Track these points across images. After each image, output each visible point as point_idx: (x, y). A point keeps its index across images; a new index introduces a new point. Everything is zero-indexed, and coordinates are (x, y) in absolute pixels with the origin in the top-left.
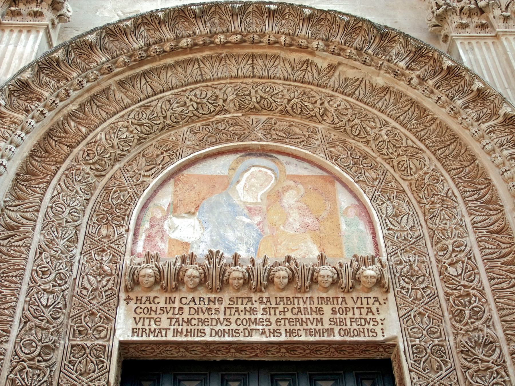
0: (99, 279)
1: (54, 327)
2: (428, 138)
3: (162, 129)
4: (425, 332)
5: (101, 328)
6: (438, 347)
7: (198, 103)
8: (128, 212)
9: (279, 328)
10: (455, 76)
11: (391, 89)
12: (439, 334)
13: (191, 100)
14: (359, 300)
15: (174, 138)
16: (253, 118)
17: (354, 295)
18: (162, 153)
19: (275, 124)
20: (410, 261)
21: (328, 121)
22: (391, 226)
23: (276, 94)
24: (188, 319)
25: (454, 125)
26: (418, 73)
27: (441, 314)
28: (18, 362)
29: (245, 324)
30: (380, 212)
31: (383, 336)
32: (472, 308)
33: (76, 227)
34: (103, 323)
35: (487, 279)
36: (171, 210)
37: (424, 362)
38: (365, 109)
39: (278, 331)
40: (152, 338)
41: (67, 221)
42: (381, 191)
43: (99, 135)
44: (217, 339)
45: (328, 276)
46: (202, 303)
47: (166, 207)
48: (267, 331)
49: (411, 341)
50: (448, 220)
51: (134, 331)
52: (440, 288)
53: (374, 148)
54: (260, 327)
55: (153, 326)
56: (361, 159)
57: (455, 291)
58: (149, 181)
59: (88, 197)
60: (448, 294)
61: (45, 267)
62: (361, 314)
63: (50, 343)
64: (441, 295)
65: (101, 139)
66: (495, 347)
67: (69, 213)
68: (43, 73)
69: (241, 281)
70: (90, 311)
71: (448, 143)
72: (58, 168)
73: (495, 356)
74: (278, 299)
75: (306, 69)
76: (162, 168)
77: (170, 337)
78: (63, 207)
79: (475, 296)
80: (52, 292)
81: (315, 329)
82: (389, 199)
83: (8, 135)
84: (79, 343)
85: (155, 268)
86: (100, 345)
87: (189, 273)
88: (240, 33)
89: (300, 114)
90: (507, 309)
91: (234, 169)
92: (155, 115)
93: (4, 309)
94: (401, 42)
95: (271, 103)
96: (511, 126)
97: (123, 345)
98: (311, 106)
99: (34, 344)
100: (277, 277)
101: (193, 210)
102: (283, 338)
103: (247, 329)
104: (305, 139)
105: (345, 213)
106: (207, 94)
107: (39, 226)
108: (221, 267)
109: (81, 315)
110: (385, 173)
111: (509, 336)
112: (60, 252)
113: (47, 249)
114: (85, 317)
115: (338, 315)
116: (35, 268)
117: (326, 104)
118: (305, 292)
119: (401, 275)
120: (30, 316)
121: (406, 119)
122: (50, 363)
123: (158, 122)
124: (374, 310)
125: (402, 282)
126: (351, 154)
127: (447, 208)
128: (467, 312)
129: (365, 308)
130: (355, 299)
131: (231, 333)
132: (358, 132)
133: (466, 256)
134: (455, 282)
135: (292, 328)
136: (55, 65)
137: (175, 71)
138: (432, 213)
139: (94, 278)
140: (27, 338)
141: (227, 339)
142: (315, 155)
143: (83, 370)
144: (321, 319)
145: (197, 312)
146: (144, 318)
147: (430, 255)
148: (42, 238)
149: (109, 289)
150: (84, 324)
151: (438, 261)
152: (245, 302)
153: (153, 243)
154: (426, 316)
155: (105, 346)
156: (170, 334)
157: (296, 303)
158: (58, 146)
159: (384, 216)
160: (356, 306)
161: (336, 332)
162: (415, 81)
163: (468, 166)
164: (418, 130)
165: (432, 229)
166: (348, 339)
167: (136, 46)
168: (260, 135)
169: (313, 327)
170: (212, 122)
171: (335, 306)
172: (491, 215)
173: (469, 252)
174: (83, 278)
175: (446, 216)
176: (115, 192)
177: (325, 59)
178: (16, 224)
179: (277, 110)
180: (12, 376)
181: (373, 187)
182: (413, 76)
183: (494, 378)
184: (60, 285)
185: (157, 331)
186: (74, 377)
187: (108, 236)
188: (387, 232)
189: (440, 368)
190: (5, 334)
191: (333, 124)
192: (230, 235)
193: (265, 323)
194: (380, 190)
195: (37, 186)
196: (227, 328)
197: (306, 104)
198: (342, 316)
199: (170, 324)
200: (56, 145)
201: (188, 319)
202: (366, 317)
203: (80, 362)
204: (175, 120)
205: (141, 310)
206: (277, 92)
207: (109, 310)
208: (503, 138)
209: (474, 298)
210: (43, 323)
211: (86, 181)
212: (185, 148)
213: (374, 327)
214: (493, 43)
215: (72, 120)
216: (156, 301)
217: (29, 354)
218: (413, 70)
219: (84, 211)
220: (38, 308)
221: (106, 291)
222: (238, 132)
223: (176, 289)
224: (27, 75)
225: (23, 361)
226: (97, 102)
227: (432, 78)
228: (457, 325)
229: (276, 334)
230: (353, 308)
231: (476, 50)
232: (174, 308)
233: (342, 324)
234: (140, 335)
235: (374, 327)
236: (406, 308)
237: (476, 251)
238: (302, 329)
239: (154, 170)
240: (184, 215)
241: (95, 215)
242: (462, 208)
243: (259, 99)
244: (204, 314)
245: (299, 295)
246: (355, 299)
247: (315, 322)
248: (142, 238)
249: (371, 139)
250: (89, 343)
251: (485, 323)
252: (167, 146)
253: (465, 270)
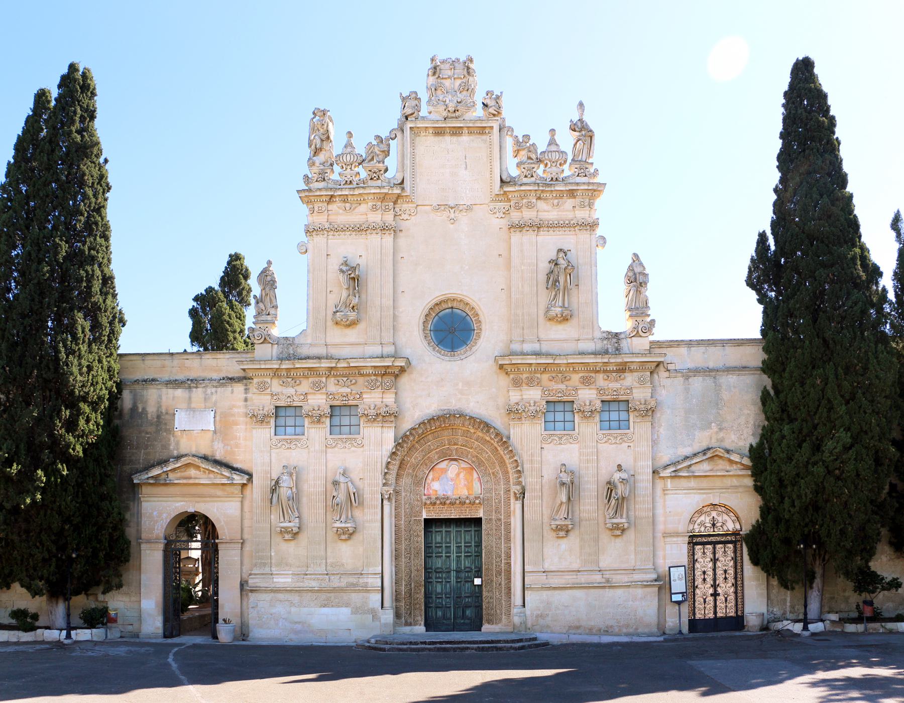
25: (504, 457)
97: (424, 519)
110: (486, 467)
192: (447, 488)
224: (394, 450)
242: (502, 483)
248: (426, 489)
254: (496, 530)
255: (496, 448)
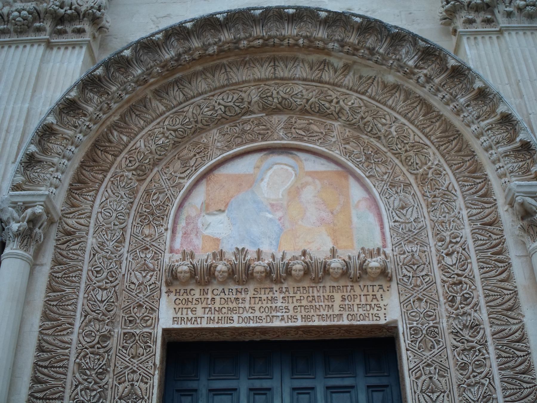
0: (144, 275)
1: (108, 319)
2: (434, 134)
3: (194, 132)
4: (422, 316)
5: (148, 318)
6: (432, 328)
7: (225, 107)
8: (166, 213)
9: (296, 314)
10: (460, 74)
11: (401, 87)
12: (434, 317)
13: (219, 104)
14: (366, 287)
15: (205, 141)
16: (275, 118)
17: (362, 284)
18: (195, 155)
19: (295, 122)
20: (412, 251)
21: (344, 118)
22: (397, 219)
23: (296, 94)
24: (219, 308)
25: (457, 122)
26: (425, 71)
27: (437, 299)
28: (82, 349)
29: (267, 311)
30: (388, 205)
31: (386, 320)
32: (463, 295)
33: (122, 229)
34: (148, 313)
35: (477, 268)
36: (204, 208)
37: (419, 342)
38: (377, 107)
39: (295, 317)
40: (189, 326)
41: (114, 225)
42: (390, 185)
43: (139, 142)
44: (243, 325)
45: (338, 268)
46: (231, 293)
47: (199, 206)
48: (286, 317)
49: (410, 324)
50: (448, 213)
51: (175, 320)
52: (438, 276)
53: (385, 144)
54: (279, 314)
55: (190, 315)
56: (373, 154)
57: (450, 279)
58: (184, 182)
59: (132, 200)
60: (444, 281)
61: (98, 267)
62: (367, 300)
63: (106, 333)
64: (439, 281)
65: (140, 146)
66: (480, 329)
67: (116, 217)
68: (87, 89)
69: (263, 275)
70: (138, 303)
71: (452, 138)
72: (105, 176)
73: (479, 337)
74: (296, 289)
75: (324, 69)
76: (195, 170)
77: (204, 325)
78: (111, 212)
79: (466, 284)
80: (106, 289)
81: (327, 315)
82: (397, 193)
83: (61, 151)
84: (129, 331)
85: (190, 265)
86: (147, 332)
87: (219, 268)
88: (263, 38)
89: (318, 112)
90: (492, 295)
91: (258, 167)
92: (187, 120)
93: (68, 305)
94: (411, 42)
95: (292, 103)
96: (507, 124)
97: (166, 331)
98: (327, 105)
99: (93, 334)
100: (294, 270)
101: (223, 209)
102: (299, 323)
103: (268, 316)
104: (322, 136)
105: (357, 206)
106: (233, 97)
107: (91, 231)
108: (246, 262)
109: (131, 307)
111: (491, 319)
112: (110, 252)
113: (99, 250)
114: (134, 308)
115: (347, 302)
116: (90, 268)
117: (341, 103)
118: (319, 282)
119: (403, 264)
120: (89, 310)
121: (414, 116)
122: (107, 349)
123: (190, 127)
124: (378, 297)
125: (404, 270)
126: (364, 150)
127: (447, 201)
128: (459, 298)
129: (371, 295)
130: (362, 287)
131: (255, 320)
132: (370, 128)
133: (461, 247)
134: (450, 271)
135: (307, 314)
136: (97, 80)
137: (204, 77)
138: (434, 206)
139: (139, 274)
140: (87, 329)
141: (252, 324)
142: (331, 152)
143: (134, 353)
144: (332, 305)
145: (226, 301)
146: (182, 308)
147: (431, 245)
148: (94, 240)
149: (153, 283)
150: (133, 314)
151: (438, 251)
152: (267, 293)
153: (189, 240)
154: (424, 301)
155: (151, 333)
156: (204, 321)
157: (311, 292)
158: (103, 156)
159: (391, 209)
160: (362, 294)
161: (345, 317)
162: (422, 79)
163: (469, 160)
164: (425, 126)
165: (433, 221)
166: (355, 323)
167: (167, 56)
168: (281, 134)
169: (325, 313)
170: (239, 123)
171: (345, 294)
172: (486, 208)
173: (464, 243)
174: (131, 274)
175: (446, 209)
176: (155, 194)
177: (340, 58)
178: (73, 230)
179: (298, 109)
180: (78, 360)
181: (382, 181)
182: (421, 75)
183: (476, 356)
184: (111, 282)
185: (193, 319)
186: (127, 359)
187: (150, 235)
188: (393, 224)
189: (433, 347)
190: (70, 326)
191: (348, 121)
193: (284, 311)
194: (389, 184)
195: (88, 194)
196: (251, 315)
197: (323, 103)
198: (350, 303)
199: (204, 313)
200: (102, 154)
201: (219, 308)
202: (371, 303)
203: (131, 347)
204: (205, 123)
205: (180, 302)
206: (297, 92)
207: (153, 302)
208: (499, 136)
209: (465, 285)
210: (100, 316)
211: (129, 186)
212: (214, 149)
213: (378, 312)
214: (498, 37)
215: (115, 129)
216: (192, 292)
217: (90, 342)
218: (421, 68)
219: (129, 214)
220: (94, 303)
221: (150, 285)
222: (262, 132)
223: (208, 283)
224: (73, 94)
225: (86, 348)
226: (135, 111)
227: (438, 76)
228: (450, 309)
229: (293, 320)
230: (360, 295)
231: (481, 45)
232: (208, 299)
233: (350, 310)
234: (179, 323)
235: (378, 312)
236: (407, 294)
237: (470, 242)
238: (315, 315)
239: (188, 172)
240: (215, 212)
241: (138, 216)
242: (460, 202)
243: (280, 100)
244: (232, 303)
245: (314, 285)
246: (362, 287)
247: (327, 309)
249: (382, 136)
250: (138, 331)
251: (473, 308)
252: (199, 148)
253: (459, 260)
254: (463, 367)
255: (422, 102)
